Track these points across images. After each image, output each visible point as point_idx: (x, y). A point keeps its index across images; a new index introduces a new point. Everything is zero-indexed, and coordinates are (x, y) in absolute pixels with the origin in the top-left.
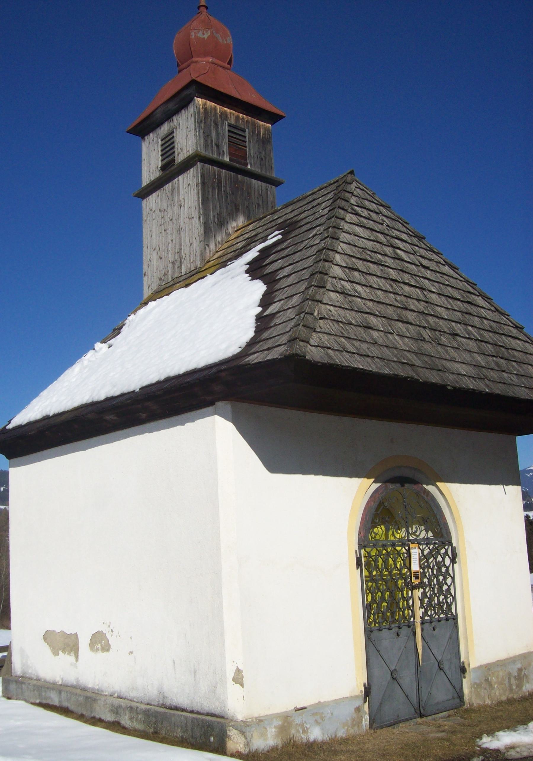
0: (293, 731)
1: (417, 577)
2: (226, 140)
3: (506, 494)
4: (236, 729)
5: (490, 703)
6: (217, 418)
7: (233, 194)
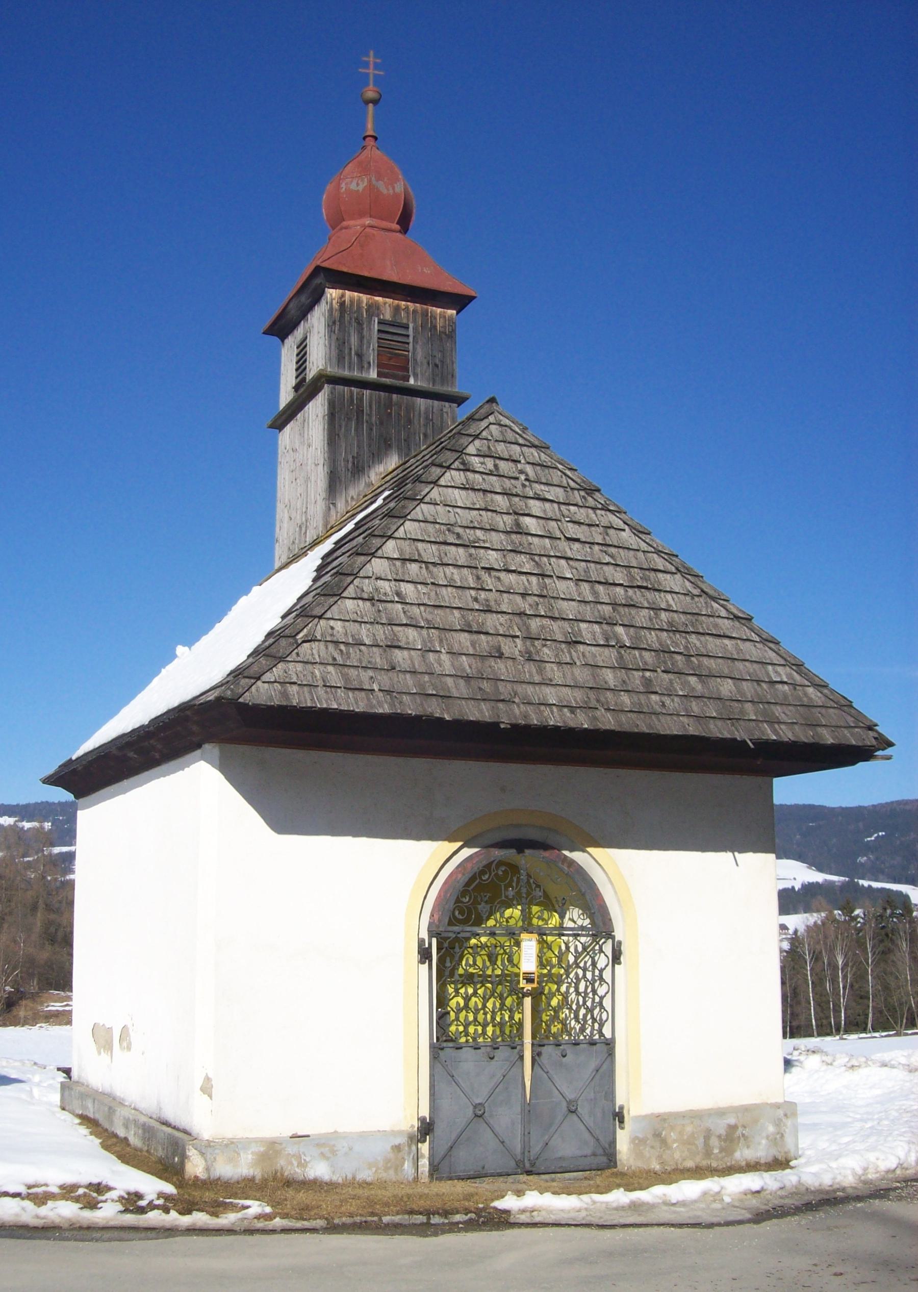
0: (282, 1162)
1: (530, 980)
2: (374, 344)
3: (737, 865)
4: (196, 1149)
5: (658, 1167)
6: (202, 764)
7: (381, 423)
